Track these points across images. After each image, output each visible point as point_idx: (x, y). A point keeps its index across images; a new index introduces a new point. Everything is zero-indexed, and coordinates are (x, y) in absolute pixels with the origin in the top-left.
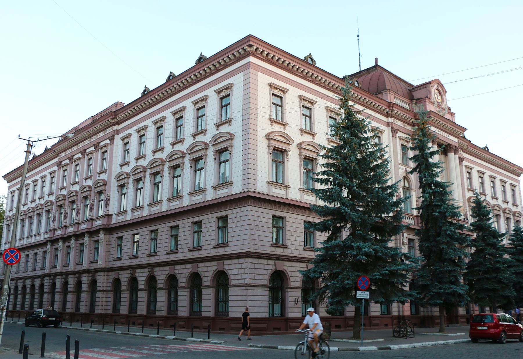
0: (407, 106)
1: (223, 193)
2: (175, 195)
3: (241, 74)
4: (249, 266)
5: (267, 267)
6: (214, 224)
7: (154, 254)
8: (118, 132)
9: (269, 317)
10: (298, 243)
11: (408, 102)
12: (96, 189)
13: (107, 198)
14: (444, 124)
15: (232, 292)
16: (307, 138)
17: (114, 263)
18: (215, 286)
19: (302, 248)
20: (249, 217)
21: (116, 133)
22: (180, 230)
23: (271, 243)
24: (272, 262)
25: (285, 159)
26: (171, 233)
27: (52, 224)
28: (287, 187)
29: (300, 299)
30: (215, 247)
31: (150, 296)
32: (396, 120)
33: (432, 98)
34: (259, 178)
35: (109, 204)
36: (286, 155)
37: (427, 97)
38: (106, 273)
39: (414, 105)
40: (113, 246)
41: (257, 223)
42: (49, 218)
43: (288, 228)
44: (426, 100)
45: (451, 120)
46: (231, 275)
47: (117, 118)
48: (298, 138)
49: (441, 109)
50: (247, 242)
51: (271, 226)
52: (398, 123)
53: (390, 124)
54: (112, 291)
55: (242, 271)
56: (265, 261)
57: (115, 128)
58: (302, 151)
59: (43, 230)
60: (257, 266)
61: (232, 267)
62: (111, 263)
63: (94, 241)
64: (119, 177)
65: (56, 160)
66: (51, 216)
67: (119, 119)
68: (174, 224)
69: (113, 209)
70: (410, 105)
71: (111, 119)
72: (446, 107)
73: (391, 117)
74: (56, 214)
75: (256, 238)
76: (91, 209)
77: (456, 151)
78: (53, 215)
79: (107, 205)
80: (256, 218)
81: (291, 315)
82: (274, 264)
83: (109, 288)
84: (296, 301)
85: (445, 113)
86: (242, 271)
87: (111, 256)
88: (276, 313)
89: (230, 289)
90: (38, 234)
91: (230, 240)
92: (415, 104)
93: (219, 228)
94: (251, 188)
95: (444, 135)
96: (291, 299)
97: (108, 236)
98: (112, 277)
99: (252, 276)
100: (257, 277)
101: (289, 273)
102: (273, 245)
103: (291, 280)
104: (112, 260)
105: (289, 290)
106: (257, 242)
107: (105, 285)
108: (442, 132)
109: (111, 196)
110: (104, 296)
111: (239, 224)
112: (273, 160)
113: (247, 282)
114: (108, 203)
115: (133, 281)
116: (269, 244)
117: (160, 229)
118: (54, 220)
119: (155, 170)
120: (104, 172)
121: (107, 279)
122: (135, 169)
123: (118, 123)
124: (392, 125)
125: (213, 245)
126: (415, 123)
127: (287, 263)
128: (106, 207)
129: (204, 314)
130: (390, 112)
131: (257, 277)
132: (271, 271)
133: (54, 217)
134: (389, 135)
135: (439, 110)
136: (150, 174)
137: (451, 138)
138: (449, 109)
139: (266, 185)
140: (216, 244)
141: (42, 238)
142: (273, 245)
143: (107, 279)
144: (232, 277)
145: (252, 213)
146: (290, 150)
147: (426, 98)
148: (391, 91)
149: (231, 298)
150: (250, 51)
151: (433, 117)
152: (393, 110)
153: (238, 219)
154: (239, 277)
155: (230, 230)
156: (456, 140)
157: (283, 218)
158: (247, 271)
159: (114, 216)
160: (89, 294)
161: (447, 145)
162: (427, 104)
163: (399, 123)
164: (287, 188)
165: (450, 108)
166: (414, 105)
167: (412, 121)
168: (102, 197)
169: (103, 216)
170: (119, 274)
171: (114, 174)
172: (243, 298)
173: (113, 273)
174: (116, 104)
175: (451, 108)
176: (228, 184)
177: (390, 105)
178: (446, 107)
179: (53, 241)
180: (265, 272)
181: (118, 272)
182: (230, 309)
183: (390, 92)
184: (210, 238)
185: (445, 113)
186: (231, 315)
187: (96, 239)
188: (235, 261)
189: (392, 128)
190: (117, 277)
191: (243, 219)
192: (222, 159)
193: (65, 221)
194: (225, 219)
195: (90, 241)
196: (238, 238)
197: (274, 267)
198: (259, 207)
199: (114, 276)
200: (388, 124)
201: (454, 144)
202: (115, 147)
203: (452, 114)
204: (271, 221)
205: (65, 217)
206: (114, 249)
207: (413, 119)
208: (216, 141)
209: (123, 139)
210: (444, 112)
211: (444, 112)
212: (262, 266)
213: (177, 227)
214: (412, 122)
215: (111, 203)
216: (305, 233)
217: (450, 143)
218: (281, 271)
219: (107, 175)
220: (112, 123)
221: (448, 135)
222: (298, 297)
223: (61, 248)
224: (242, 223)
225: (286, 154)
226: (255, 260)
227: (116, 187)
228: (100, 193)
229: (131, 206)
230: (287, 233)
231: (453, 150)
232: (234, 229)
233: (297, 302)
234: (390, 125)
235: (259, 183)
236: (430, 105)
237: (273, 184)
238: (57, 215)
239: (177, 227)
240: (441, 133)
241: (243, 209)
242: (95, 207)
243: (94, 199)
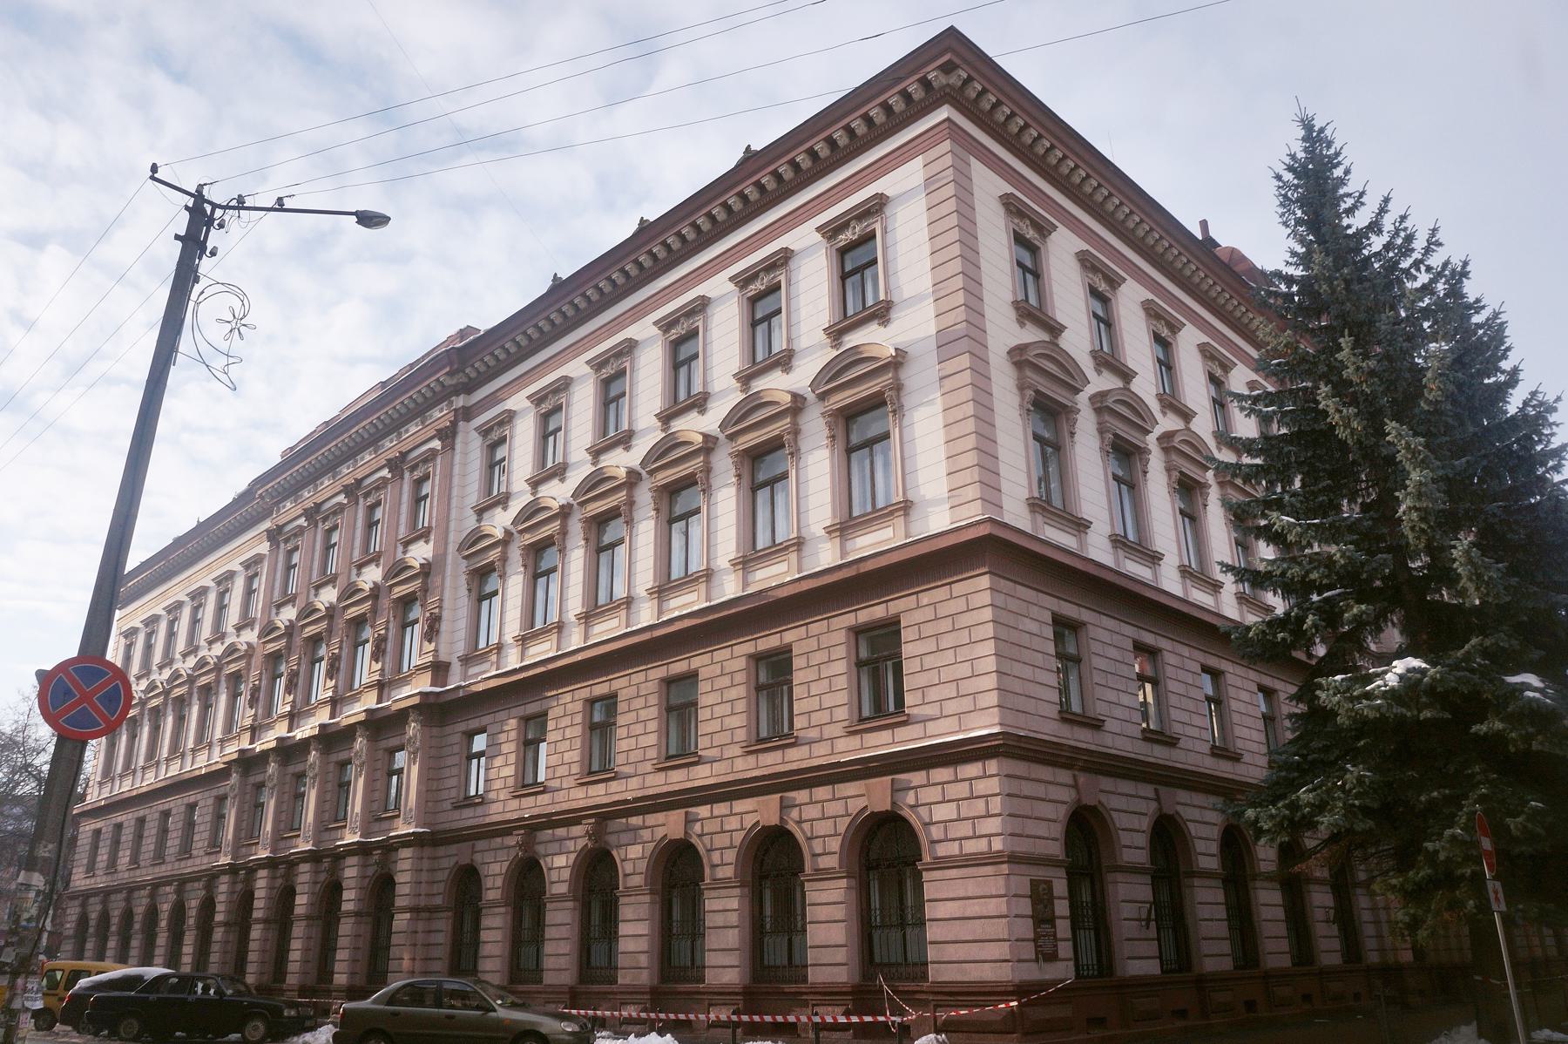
3: (919, 162)
6: (841, 651)
8: (467, 414)
13: (431, 614)
17: (456, 814)
18: (857, 869)
21: (461, 416)
22: (703, 687)
26: (668, 701)
31: (589, 922)
35: (438, 631)
38: (428, 851)
40: (450, 761)
47: (467, 371)
54: (448, 910)
56: (1045, 772)
57: (460, 401)
61: (931, 794)
62: (442, 817)
63: (386, 750)
65: (267, 525)
67: (473, 375)
68: (679, 667)
69: (453, 643)
71: (447, 374)
79: (432, 633)
82: (1071, 782)
83: (438, 901)
87: (445, 795)
88: (1090, 962)
93: (860, 664)
97: (435, 731)
98: (448, 863)
103: (1124, 842)
104: (450, 807)
107: (424, 888)
110: (421, 926)
114: (437, 626)
115: (528, 873)
117: (625, 691)
120: (425, 535)
121: (432, 870)
123: (469, 388)
129: (816, 976)
143: (432, 870)
149: (931, 911)
150: (948, 85)
159: (456, 668)
160: (366, 923)
168: (416, 612)
170: (474, 852)
171: (455, 538)
173: (453, 849)
174: (463, 333)
181: (471, 843)
184: (828, 701)
190: (467, 861)
195: (372, 750)
198: (1015, 582)
199: (453, 861)
202: (457, 458)
206: (455, 771)
208: (833, 376)
209: (485, 432)
213: (692, 677)
215: (444, 626)
218: (1095, 808)
219: (431, 543)
220: (451, 386)
223: (275, 781)
228: (407, 602)
230: (1097, 678)
239: (692, 677)
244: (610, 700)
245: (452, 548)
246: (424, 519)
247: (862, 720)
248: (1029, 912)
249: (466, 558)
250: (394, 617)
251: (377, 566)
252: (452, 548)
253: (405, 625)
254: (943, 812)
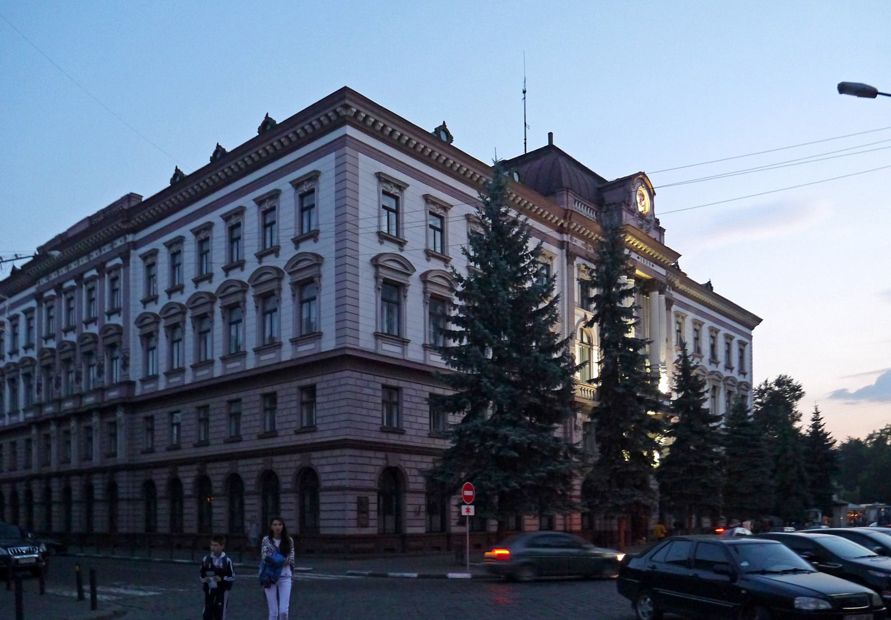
1: (306, 349)
2: (233, 351)
4: (347, 460)
5: (374, 462)
6: (294, 398)
7: (205, 443)
9: (378, 533)
10: (419, 427)
11: (594, 208)
12: (105, 341)
15: (323, 498)
16: (436, 265)
19: (425, 434)
20: (348, 388)
23: (381, 426)
24: (381, 455)
25: (403, 298)
27: (36, 396)
28: (404, 342)
29: (423, 508)
30: (297, 433)
32: (575, 238)
33: (632, 204)
34: (361, 327)
36: (404, 292)
37: (624, 202)
39: (603, 214)
41: (359, 396)
42: (29, 387)
43: (405, 405)
44: (623, 207)
45: (658, 239)
46: (322, 473)
48: (421, 265)
49: (644, 221)
50: (344, 424)
51: (380, 401)
52: (578, 243)
53: (565, 243)
55: (337, 468)
56: (371, 454)
58: (429, 285)
59: (22, 405)
60: (360, 461)
61: (323, 462)
64: (141, 321)
66: (35, 383)
69: (136, 373)
70: (598, 214)
72: (653, 219)
73: (567, 234)
74: (41, 379)
75: (358, 418)
76: (100, 373)
78: (36, 382)
79: (125, 366)
80: (358, 390)
81: (410, 530)
84: (418, 510)
85: (650, 227)
86: (337, 468)
89: (321, 494)
90: (14, 412)
91: (319, 421)
92: (605, 212)
93: (302, 403)
94: (350, 342)
96: (409, 508)
99: (353, 476)
100: (360, 476)
101: (408, 471)
102: (383, 430)
103: (410, 480)
105: (408, 495)
106: (359, 425)
109: (131, 351)
111: (332, 398)
112: (383, 299)
113: (345, 483)
116: (377, 428)
118: (39, 390)
119: (200, 311)
122: (168, 308)
124: (568, 246)
125: (295, 429)
127: (406, 457)
128: (125, 370)
130: (565, 225)
131: (360, 476)
132: (379, 467)
133: (39, 385)
134: (562, 262)
135: (641, 222)
136: (192, 318)
138: (657, 221)
139: (372, 339)
140: (299, 428)
141: (21, 418)
142: (383, 430)
144: (323, 477)
145: (351, 381)
146: (409, 283)
147: (623, 204)
152: (570, 224)
153: (331, 391)
154: (332, 477)
155: (318, 407)
157: (398, 389)
158: (346, 468)
162: (624, 213)
163: (579, 243)
164: (405, 344)
165: (658, 220)
166: (603, 214)
168: (117, 353)
169: (120, 384)
172: (340, 507)
175: (660, 221)
176: (314, 337)
177: (567, 214)
178: (653, 219)
179: (41, 424)
180: (371, 469)
182: (322, 524)
185: (650, 227)
186: (324, 532)
187: (111, 419)
188: (327, 453)
189: (567, 251)
191: (339, 389)
192: (305, 296)
193: (58, 391)
194: (311, 390)
196: (330, 419)
197: (385, 462)
200: (562, 245)
203: (662, 231)
204: (379, 393)
205: (58, 385)
210: (648, 227)
211: (648, 227)
212: (367, 461)
215: (131, 363)
216: (432, 412)
218: (396, 468)
222: (420, 505)
224: (337, 397)
225: (404, 290)
226: (356, 452)
227: (139, 338)
228: (112, 347)
229: (163, 368)
230: (405, 412)
232: (326, 406)
233: (419, 512)
234: (565, 246)
235: (362, 336)
236: (628, 215)
237: (382, 337)
238: (43, 382)
241: (338, 375)
242: (106, 369)
243: (104, 356)
244: (206, 407)
245: (132, 321)
246: (120, 302)
247: (302, 428)
248: (356, 509)
249: (140, 327)
250: (107, 355)
251: (96, 324)
252: (132, 321)
253: (112, 359)
254: (328, 469)
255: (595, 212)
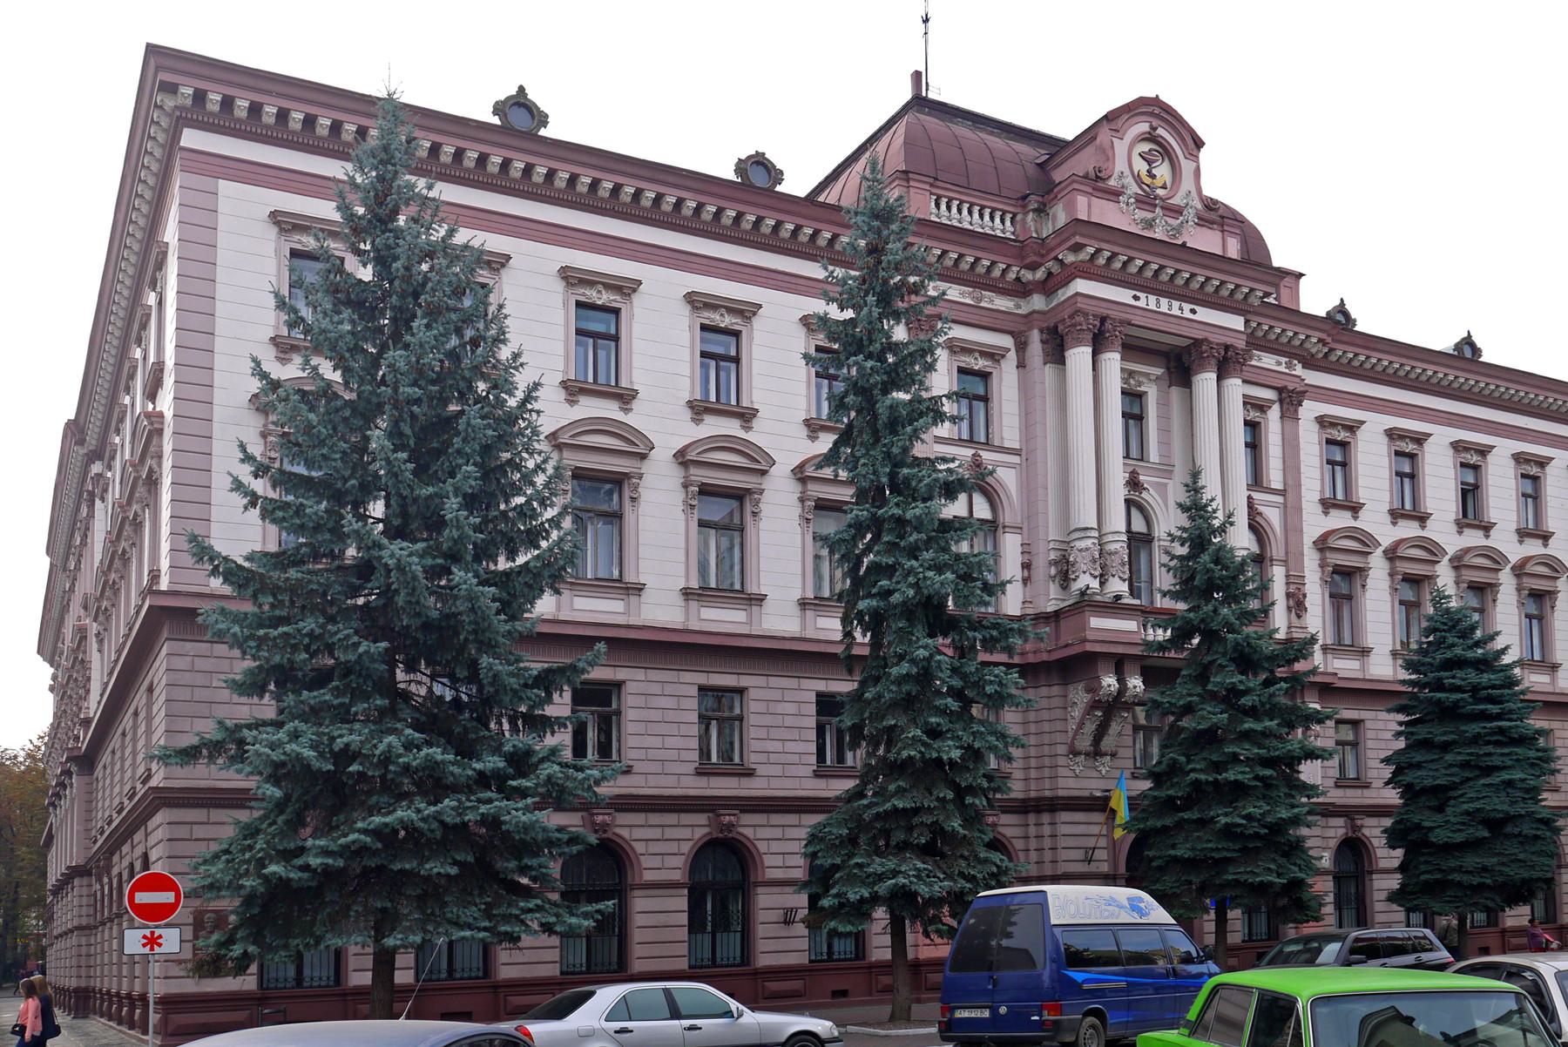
0: (1001, 228)
14: (1155, 267)
39: (1030, 215)
70: (1019, 217)
77: (1227, 362)
95: (1152, 306)
108: (1152, 298)
126: (1029, 282)
137: (1206, 315)
148: (911, 175)
151: (1092, 242)
156: (1237, 322)
161: (1188, 349)
167: (1014, 276)
183: (908, 180)
201: (1217, 338)
207: (1015, 269)
214: (1018, 279)
217: (1199, 335)
221: (1187, 307)
231: (1214, 362)
240: (1149, 301)
255: (1008, 217)
